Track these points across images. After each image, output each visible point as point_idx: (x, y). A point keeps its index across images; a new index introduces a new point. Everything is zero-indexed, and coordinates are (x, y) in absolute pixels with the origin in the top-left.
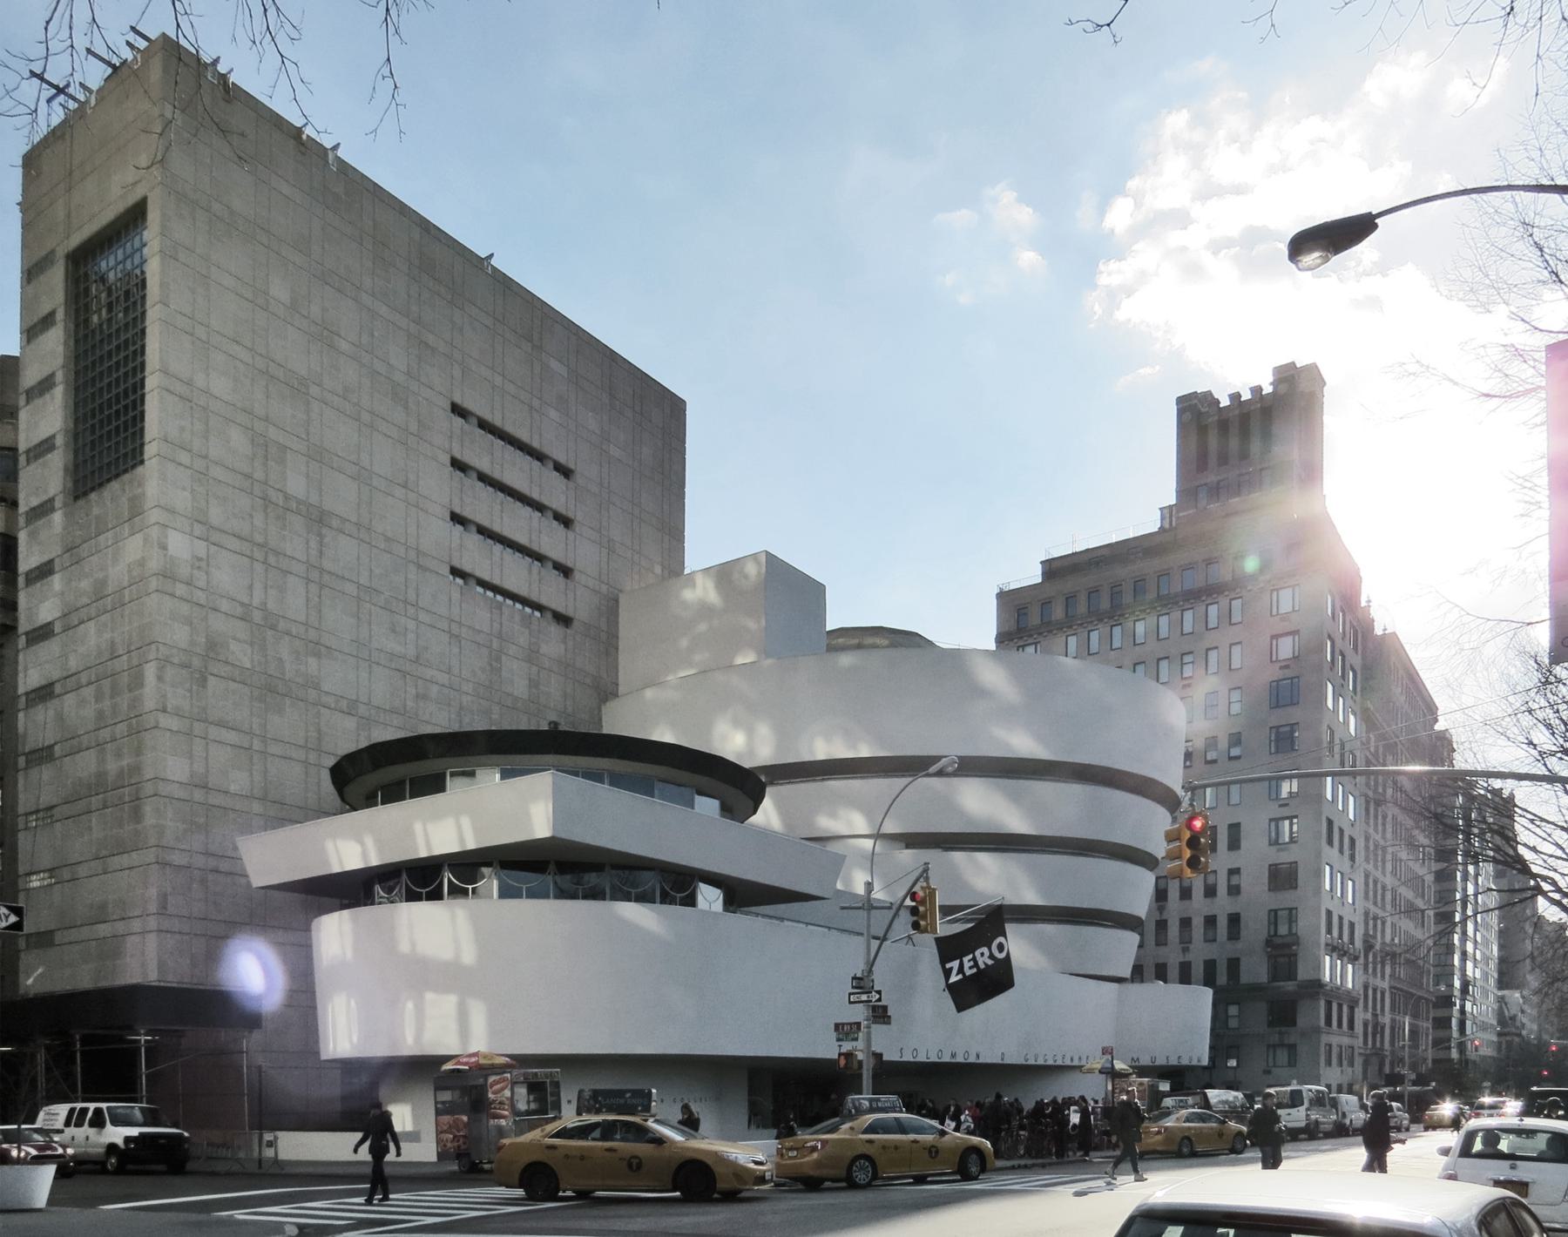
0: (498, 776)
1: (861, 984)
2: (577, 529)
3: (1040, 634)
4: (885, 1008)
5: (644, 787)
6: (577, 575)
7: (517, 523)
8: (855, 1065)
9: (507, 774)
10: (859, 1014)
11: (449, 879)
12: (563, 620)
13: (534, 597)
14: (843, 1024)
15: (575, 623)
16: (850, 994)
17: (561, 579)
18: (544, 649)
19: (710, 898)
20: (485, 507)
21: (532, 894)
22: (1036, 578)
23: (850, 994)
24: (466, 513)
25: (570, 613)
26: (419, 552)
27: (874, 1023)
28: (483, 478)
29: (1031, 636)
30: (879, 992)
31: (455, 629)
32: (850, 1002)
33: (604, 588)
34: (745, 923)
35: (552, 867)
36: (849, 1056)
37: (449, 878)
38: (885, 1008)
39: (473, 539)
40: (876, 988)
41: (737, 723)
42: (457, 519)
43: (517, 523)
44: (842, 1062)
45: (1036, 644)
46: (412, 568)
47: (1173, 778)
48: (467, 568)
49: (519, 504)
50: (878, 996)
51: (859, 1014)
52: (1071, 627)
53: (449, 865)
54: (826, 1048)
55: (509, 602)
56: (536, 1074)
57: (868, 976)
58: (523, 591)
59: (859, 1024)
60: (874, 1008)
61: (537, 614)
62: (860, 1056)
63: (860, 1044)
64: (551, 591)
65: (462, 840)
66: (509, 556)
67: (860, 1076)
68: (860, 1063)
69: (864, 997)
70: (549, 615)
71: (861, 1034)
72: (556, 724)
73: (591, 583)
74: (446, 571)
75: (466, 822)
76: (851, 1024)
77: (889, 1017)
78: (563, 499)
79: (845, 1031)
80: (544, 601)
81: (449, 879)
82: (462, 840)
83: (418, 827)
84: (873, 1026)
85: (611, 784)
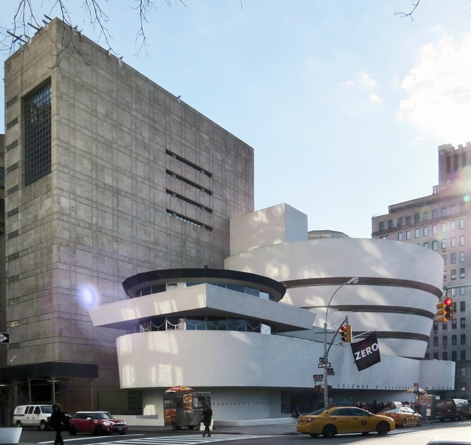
0: (185, 285)
1: (323, 360)
2: (214, 195)
3: (389, 232)
4: (332, 369)
5: (240, 289)
6: (214, 212)
7: (191, 193)
8: (321, 391)
9: (188, 285)
10: (322, 371)
11: (168, 323)
13: (198, 220)
14: (316, 375)
15: (214, 230)
16: (319, 364)
17: (208, 214)
18: (202, 239)
19: (266, 329)
20: (178, 187)
21: (200, 328)
22: (387, 213)
23: (319, 364)
24: (172, 190)
25: (212, 226)
26: (154, 204)
27: (328, 375)
28: (179, 177)
29: (385, 233)
30: (330, 364)
31: (168, 231)
32: (319, 367)
33: (224, 217)
34: (279, 339)
35: (206, 318)
36: (319, 387)
37: (168, 323)
38: (332, 369)
39: (175, 200)
40: (329, 362)
41: (274, 266)
42: (168, 192)
43: (191, 193)
44: (317, 389)
45: (387, 236)
46: (152, 210)
47: (439, 285)
48: (173, 209)
50: (329, 365)
51: (322, 371)
52: (400, 230)
53: (168, 318)
54: (310, 384)
55: (189, 222)
56: (201, 394)
57: (326, 358)
58: (194, 218)
59: (322, 375)
60: (328, 369)
61: (199, 226)
62: (323, 387)
63: (323, 383)
64: (204, 218)
65: (172, 308)
67: (323, 394)
68: (323, 389)
69: (324, 365)
70: (204, 227)
71: (323, 379)
72: (207, 266)
73: (219, 215)
74: (165, 210)
75: (174, 302)
76: (319, 375)
77: (334, 373)
78: (208, 184)
79: (317, 378)
80: (202, 221)
81: (168, 323)
82: (172, 308)
83: (156, 304)
84: (328, 376)
85: (228, 288)
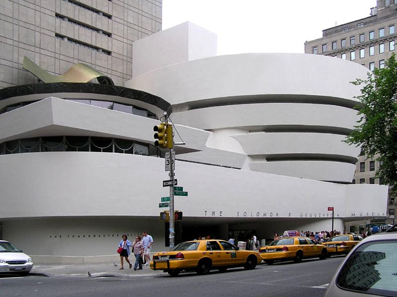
12: (109, 53)
13: (94, 44)
17: (107, 36)
25: (110, 50)
33: (125, 41)
39: (65, 23)
49: (87, 10)
54: (156, 212)
58: (89, 42)
66: (82, 29)
70: (101, 50)
73: (119, 38)
74: (54, 35)
80: (98, 45)
